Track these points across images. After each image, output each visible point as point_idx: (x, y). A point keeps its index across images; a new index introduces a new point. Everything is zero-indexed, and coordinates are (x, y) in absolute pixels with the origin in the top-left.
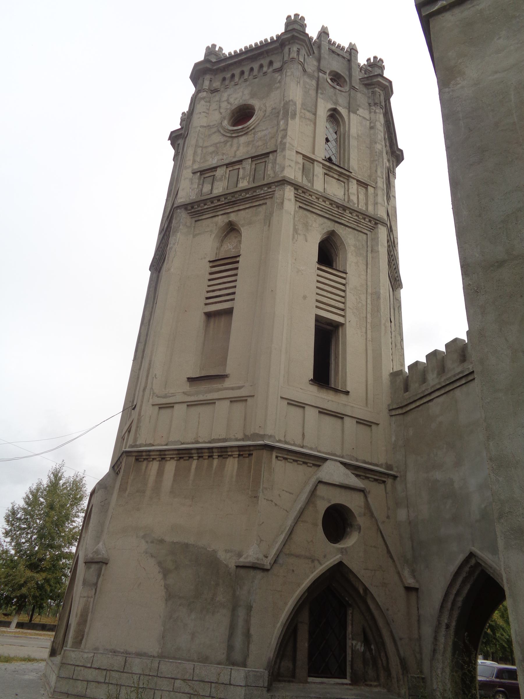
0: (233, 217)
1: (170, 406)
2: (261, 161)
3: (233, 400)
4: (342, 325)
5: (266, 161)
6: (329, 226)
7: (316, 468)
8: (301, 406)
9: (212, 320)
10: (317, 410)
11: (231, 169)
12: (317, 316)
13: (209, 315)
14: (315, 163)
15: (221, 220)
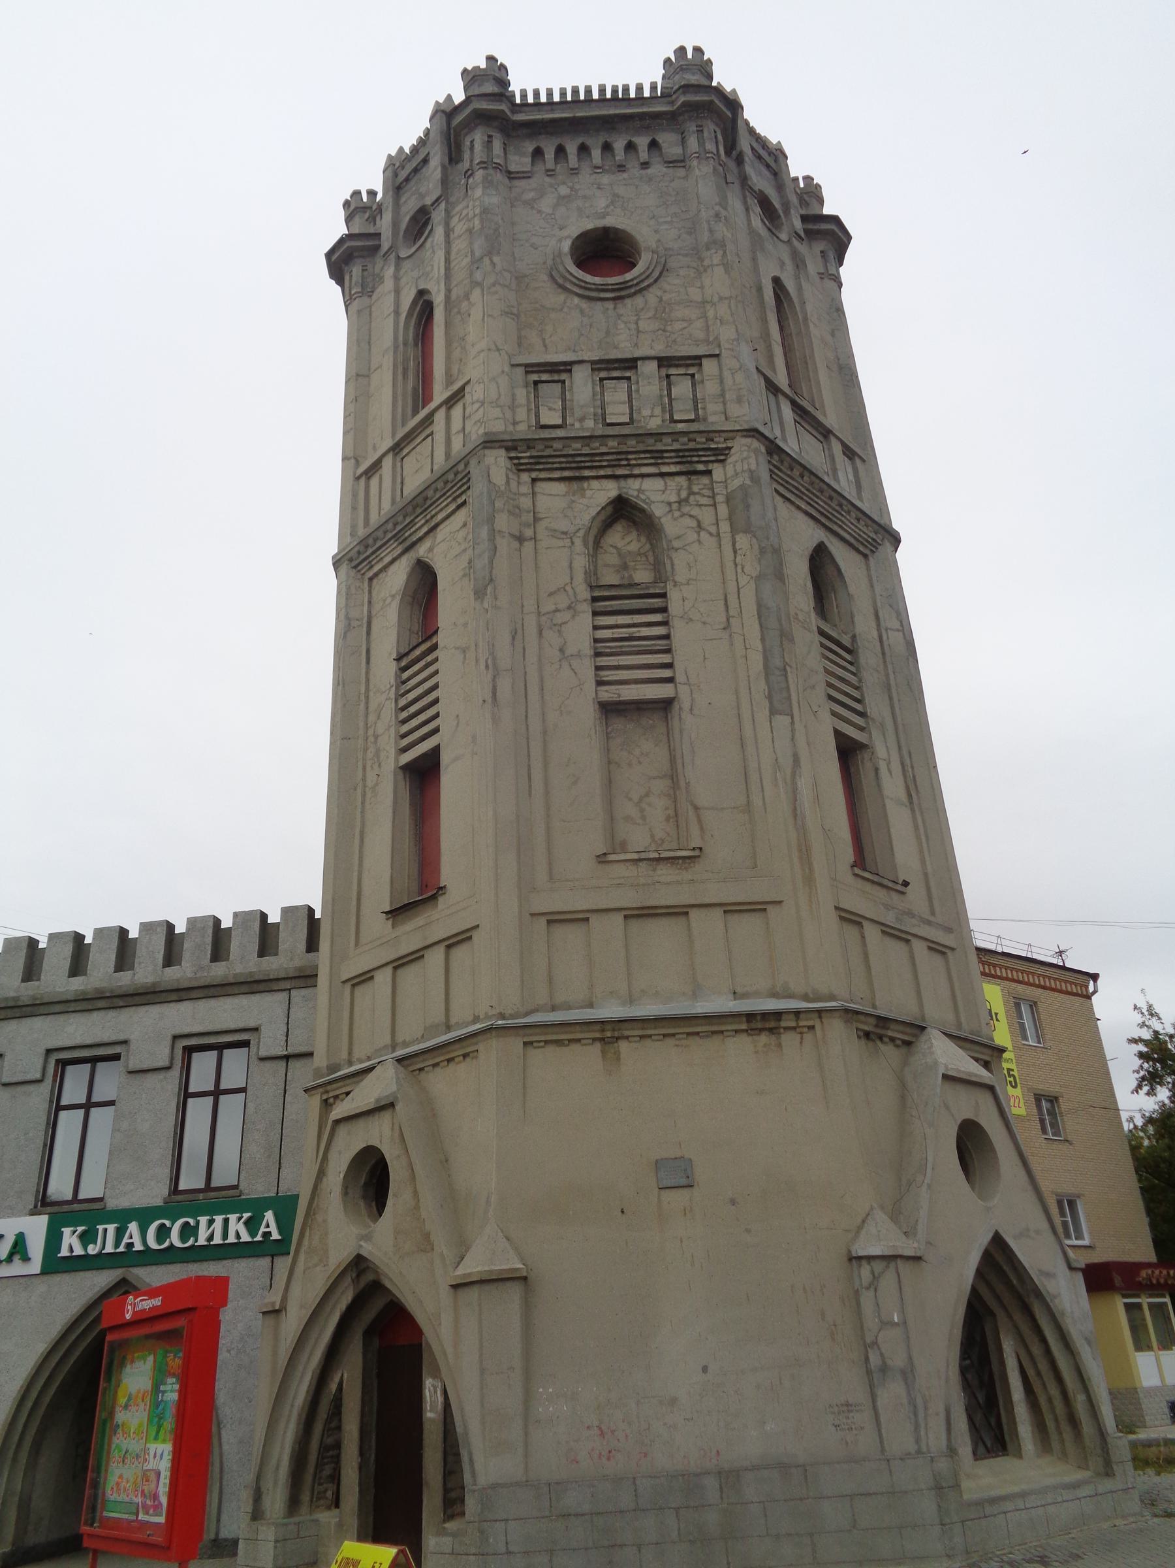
0: (632, 488)
1: (580, 919)
2: (682, 371)
3: (732, 909)
4: (862, 746)
5: (693, 376)
6: (820, 535)
7: (904, 1050)
8: (850, 918)
9: (618, 723)
10: (878, 928)
11: (603, 374)
12: (837, 733)
13: (610, 710)
14: (781, 397)
15: (602, 493)
